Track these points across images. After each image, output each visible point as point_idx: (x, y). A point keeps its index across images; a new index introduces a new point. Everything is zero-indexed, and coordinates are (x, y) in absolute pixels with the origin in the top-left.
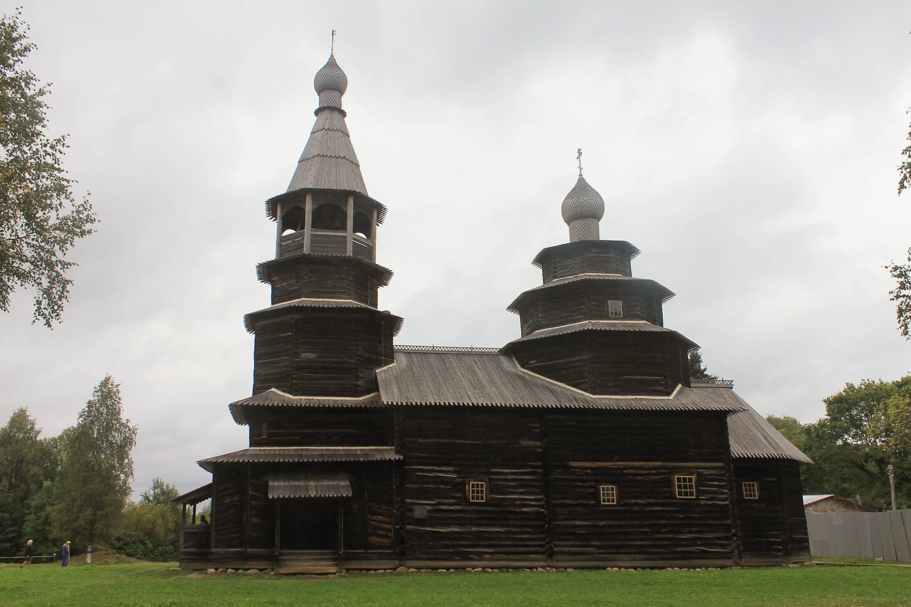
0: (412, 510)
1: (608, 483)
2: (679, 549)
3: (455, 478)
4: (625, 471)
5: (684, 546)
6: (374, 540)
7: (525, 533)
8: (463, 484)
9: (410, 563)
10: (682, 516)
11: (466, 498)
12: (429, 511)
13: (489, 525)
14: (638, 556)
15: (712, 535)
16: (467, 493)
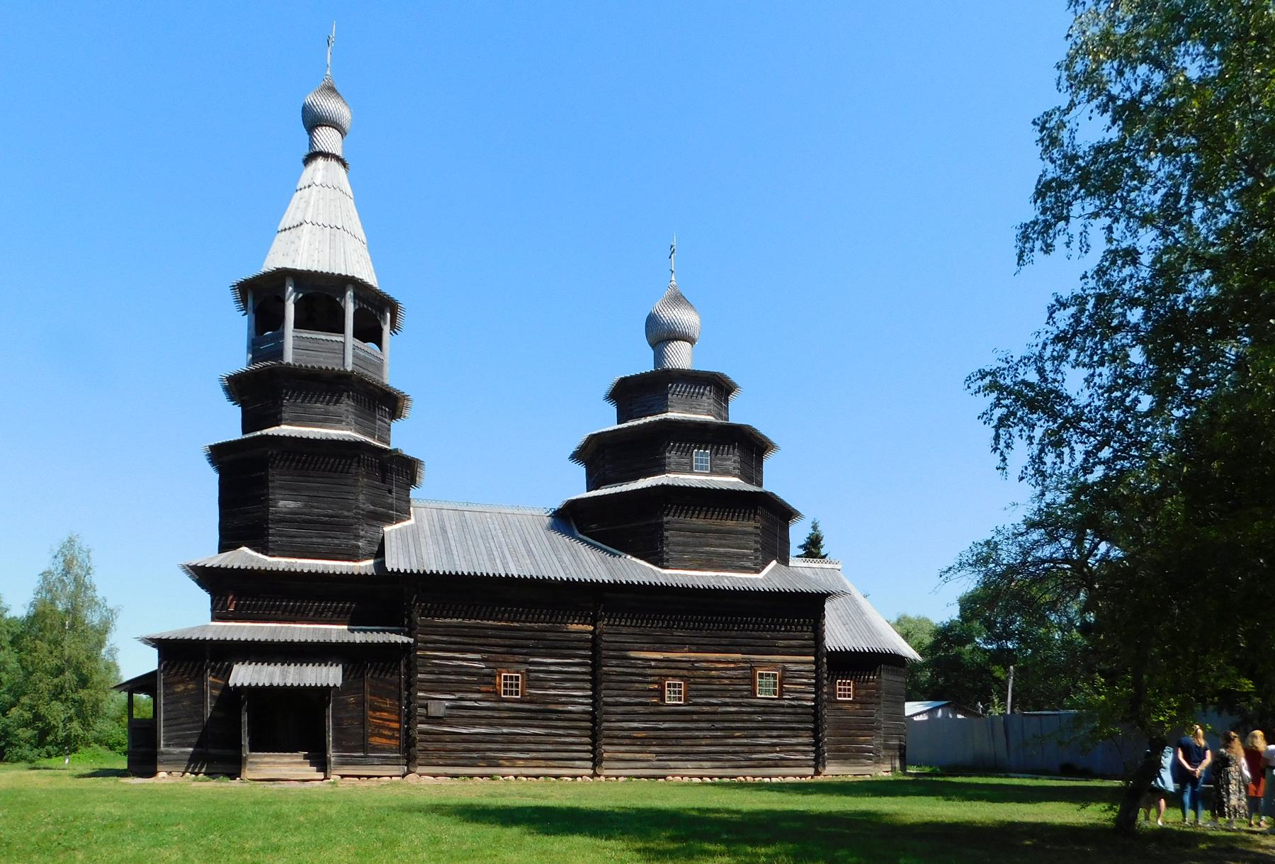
0: (426, 707)
1: (674, 677)
2: (754, 756)
4: (696, 665)
5: (761, 752)
6: (376, 741)
8: (493, 676)
9: (420, 770)
11: (497, 693)
12: (447, 708)
15: (794, 741)
16: (498, 687)
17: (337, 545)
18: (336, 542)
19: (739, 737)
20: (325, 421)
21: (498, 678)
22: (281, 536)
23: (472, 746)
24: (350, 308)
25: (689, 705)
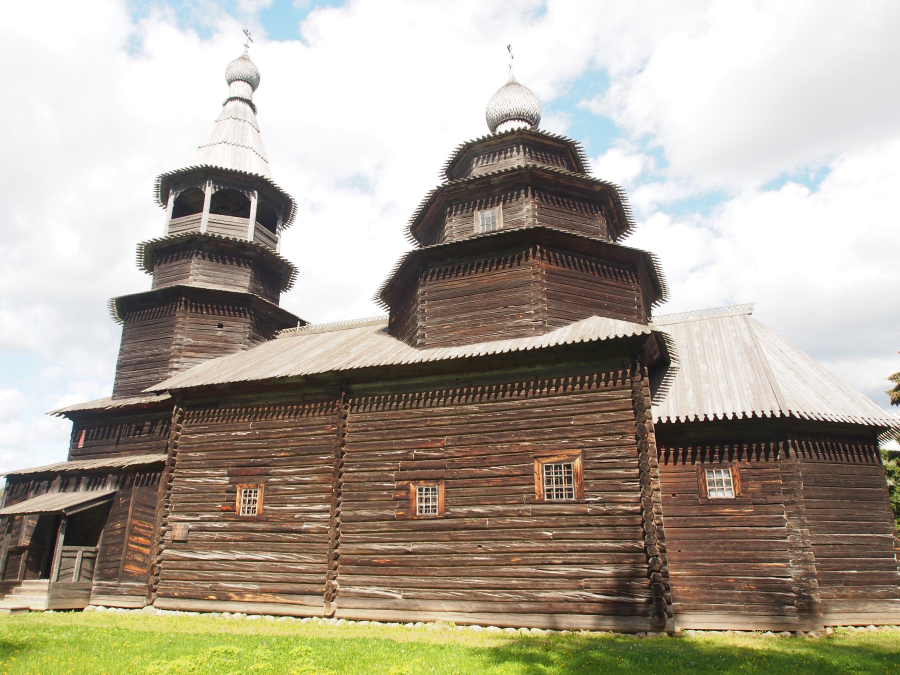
2: (542, 595)
6: (132, 569)
9: (158, 602)
10: (549, 534)
13: (257, 551)
14: (467, 606)
18: (157, 376)
19: (518, 564)
21: (238, 494)
24: (209, 191)
25: (447, 517)
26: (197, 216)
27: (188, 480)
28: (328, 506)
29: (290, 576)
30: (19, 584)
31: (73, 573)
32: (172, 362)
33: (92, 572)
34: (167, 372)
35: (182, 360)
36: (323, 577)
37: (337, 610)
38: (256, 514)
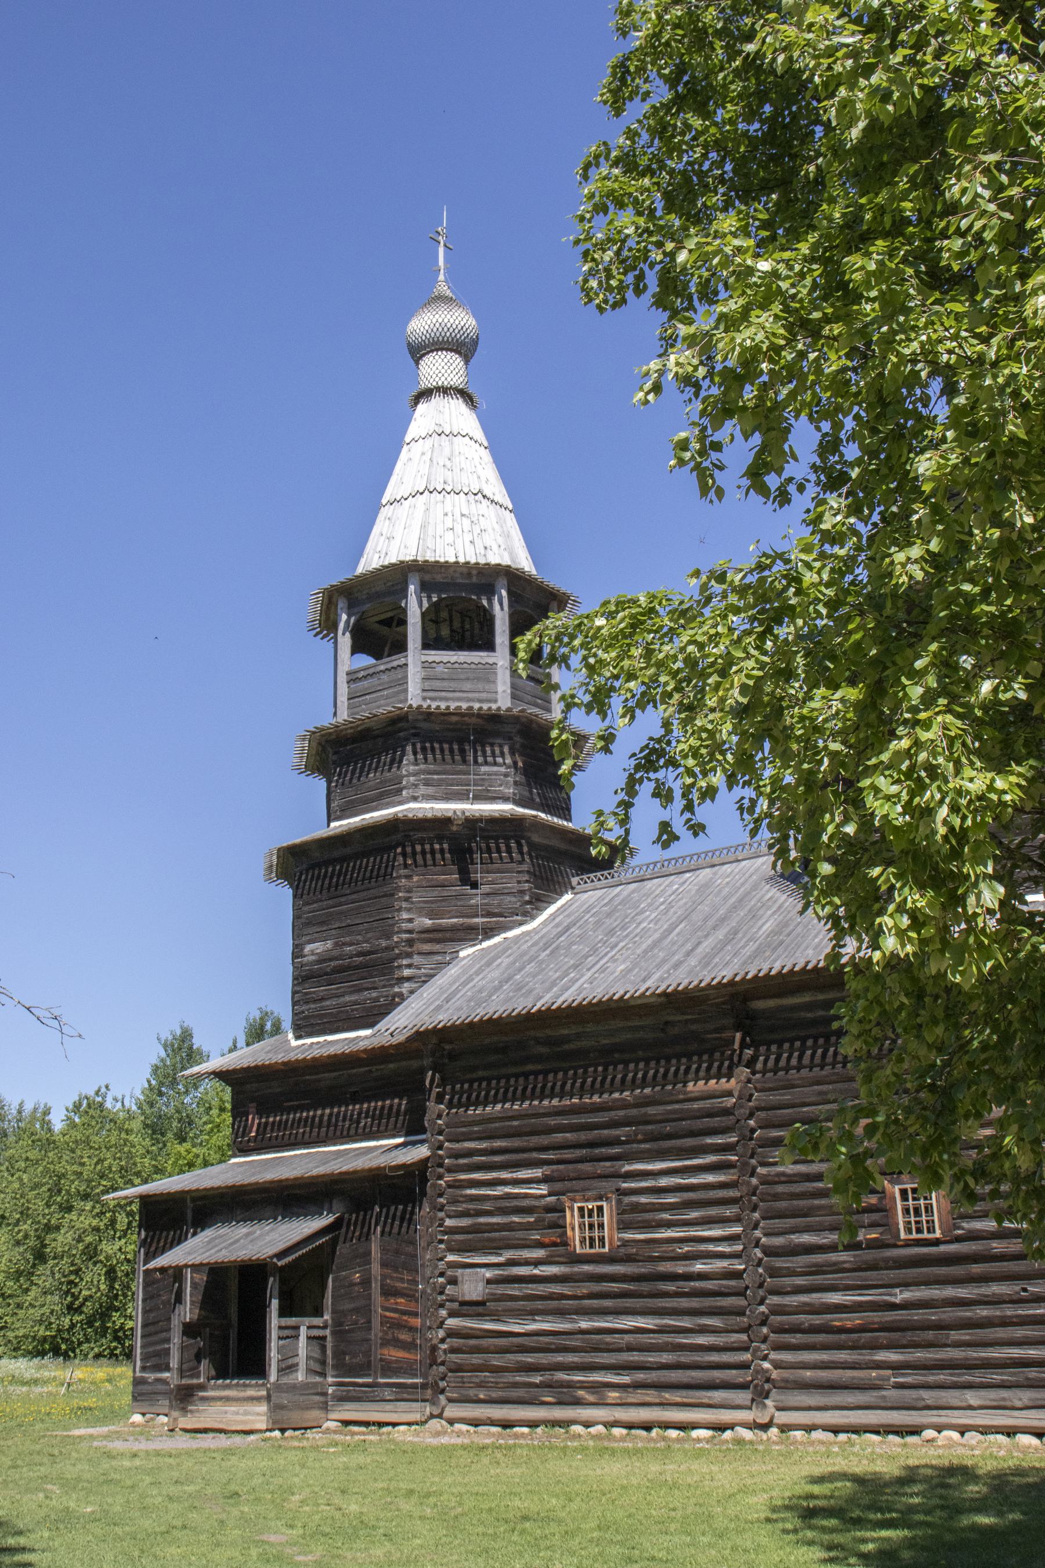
3: (543, 1196)
7: (703, 1330)
12: (489, 1282)
16: (569, 1233)
17: (376, 999)
18: (374, 994)
20: (380, 797)
22: (307, 1003)
23: (529, 1359)
24: (414, 607)
25: (958, 1239)
26: (397, 660)
27: (469, 1192)
28: (737, 1229)
29: (686, 1358)
30: (202, 1387)
31: (297, 1364)
32: (400, 967)
33: (323, 1363)
34: (392, 986)
35: (417, 959)
36: (747, 1356)
37: (777, 1414)
38: (606, 1250)
